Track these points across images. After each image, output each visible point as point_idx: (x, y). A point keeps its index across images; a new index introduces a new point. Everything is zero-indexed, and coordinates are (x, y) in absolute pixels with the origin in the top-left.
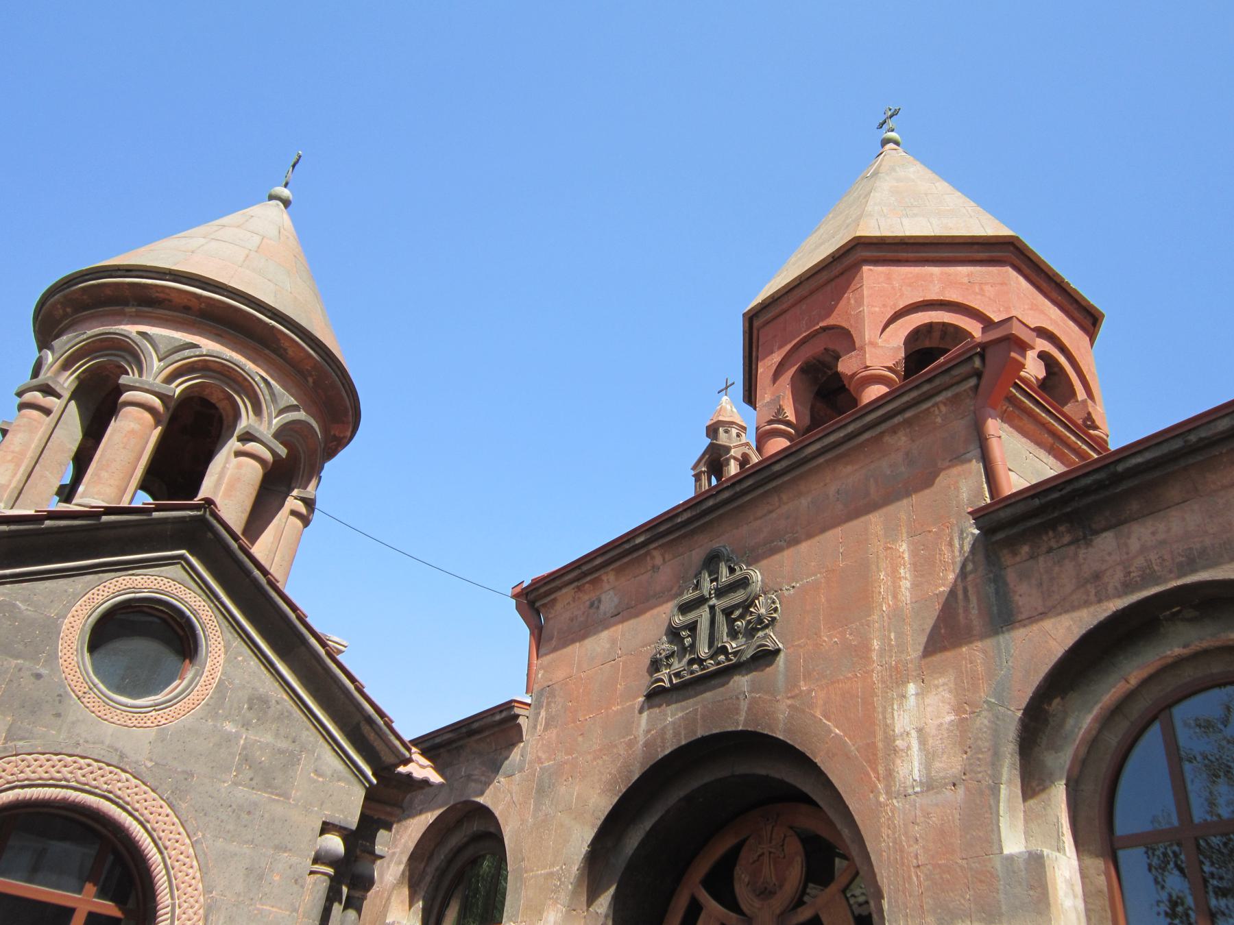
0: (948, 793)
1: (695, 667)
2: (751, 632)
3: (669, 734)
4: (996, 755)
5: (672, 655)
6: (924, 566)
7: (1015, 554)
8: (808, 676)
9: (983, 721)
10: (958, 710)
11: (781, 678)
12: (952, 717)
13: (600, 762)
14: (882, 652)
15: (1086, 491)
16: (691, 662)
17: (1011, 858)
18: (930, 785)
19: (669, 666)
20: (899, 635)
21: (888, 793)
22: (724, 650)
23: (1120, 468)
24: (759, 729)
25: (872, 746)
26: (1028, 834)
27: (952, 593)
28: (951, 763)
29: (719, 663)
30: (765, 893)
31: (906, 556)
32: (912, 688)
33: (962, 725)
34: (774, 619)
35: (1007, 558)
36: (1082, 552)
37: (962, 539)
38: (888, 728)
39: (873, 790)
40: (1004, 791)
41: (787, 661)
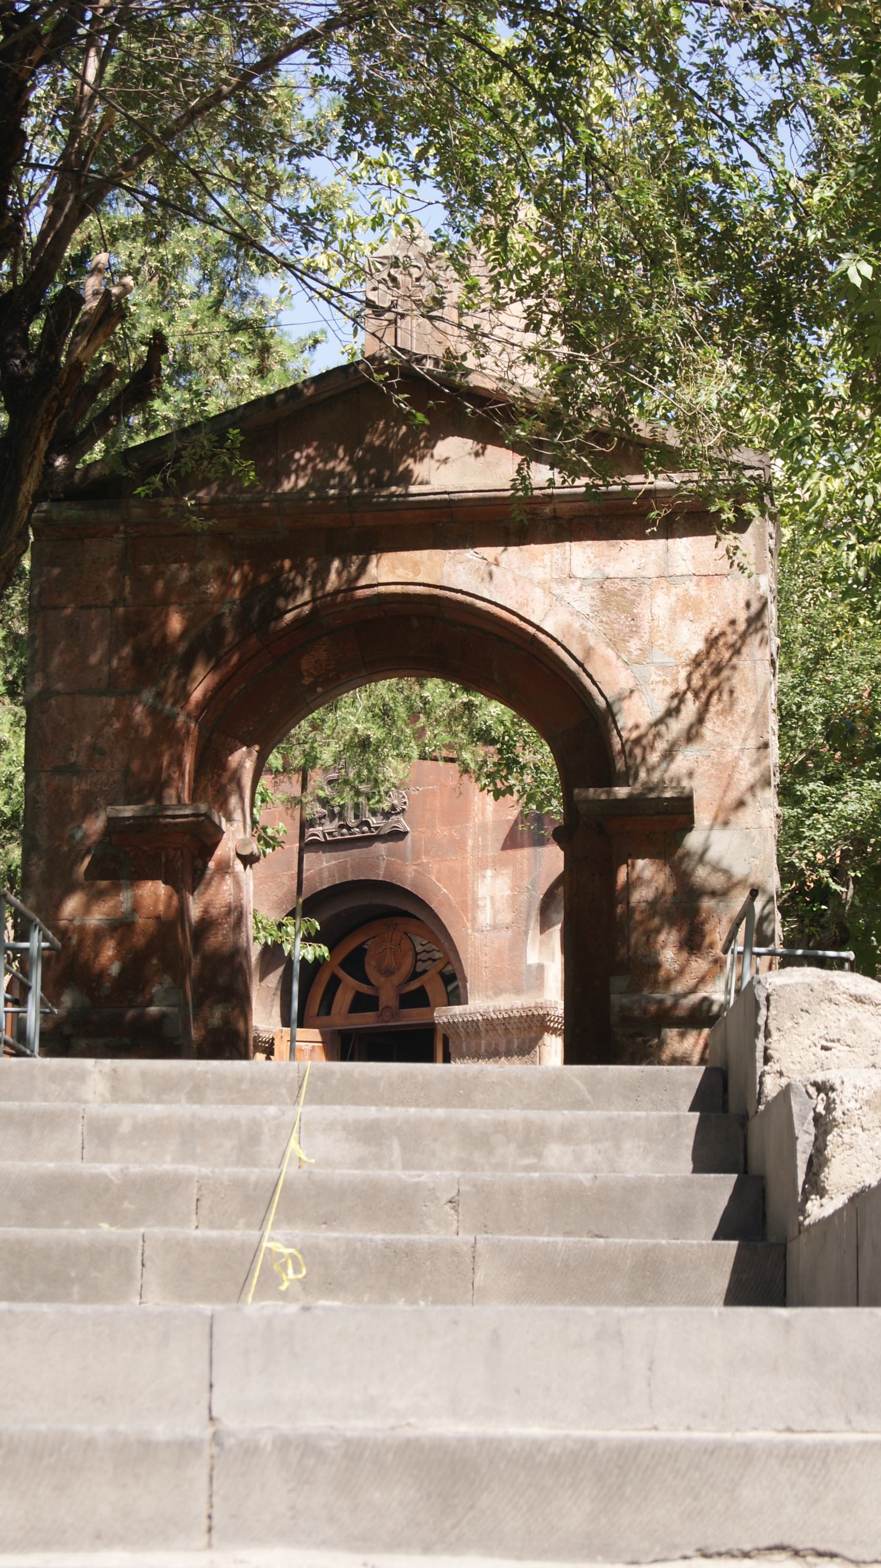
1: (344, 831)
2: (387, 815)
3: (326, 874)
4: (529, 916)
5: (324, 817)
8: (427, 853)
9: (524, 897)
10: (513, 889)
11: (409, 851)
12: (508, 892)
13: (267, 887)
14: (473, 848)
16: (341, 827)
17: (530, 966)
18: (495, 927)
19: (322, 824)
20: (484, 839)
21: (473, 929)
22: (367, 823)
24: (394, 881)
25: (465, 902)
26: (540, 953)
28: (506, 917)
29: (363, 832)
30: (388, 973)
32: (489, 873)
33: (514, 897)
34: (403, 810)
39: (465, 926)
40: (531, 933)
41: (414, 841)
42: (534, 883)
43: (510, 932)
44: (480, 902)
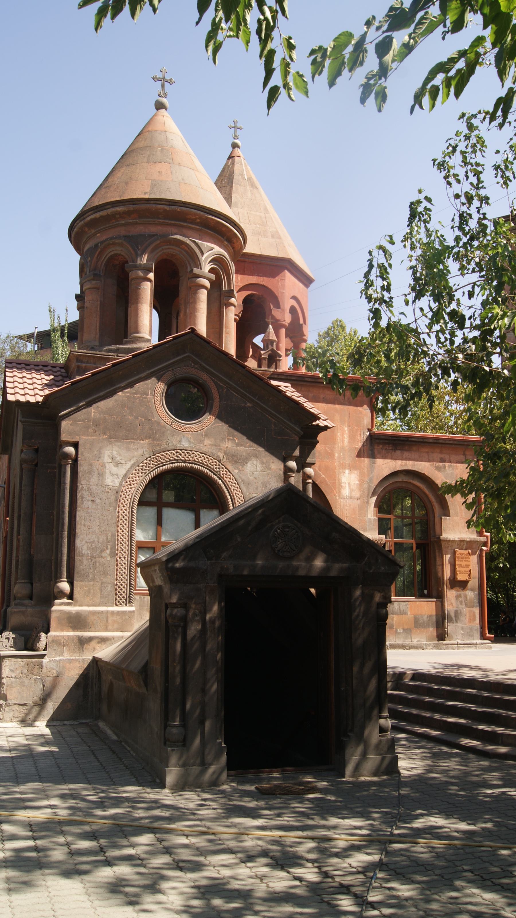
0: (356, 500)
6: (352, 438)
7: (378, 446)
9: (366, 486)
10: (359, 481)
14: (339, 457)
15: (399, 440)
18: (351, 498)
23: (410, 439)
25: (335, 483)
27: (360, 449)
28: (357, 494)
31: (347, 432)
35: (376, 446)
36: (393, 453)
37: (364, 435)
38: (340, 481)
42: (371, 480)
43: (359, 501)
44: (342, 484)
